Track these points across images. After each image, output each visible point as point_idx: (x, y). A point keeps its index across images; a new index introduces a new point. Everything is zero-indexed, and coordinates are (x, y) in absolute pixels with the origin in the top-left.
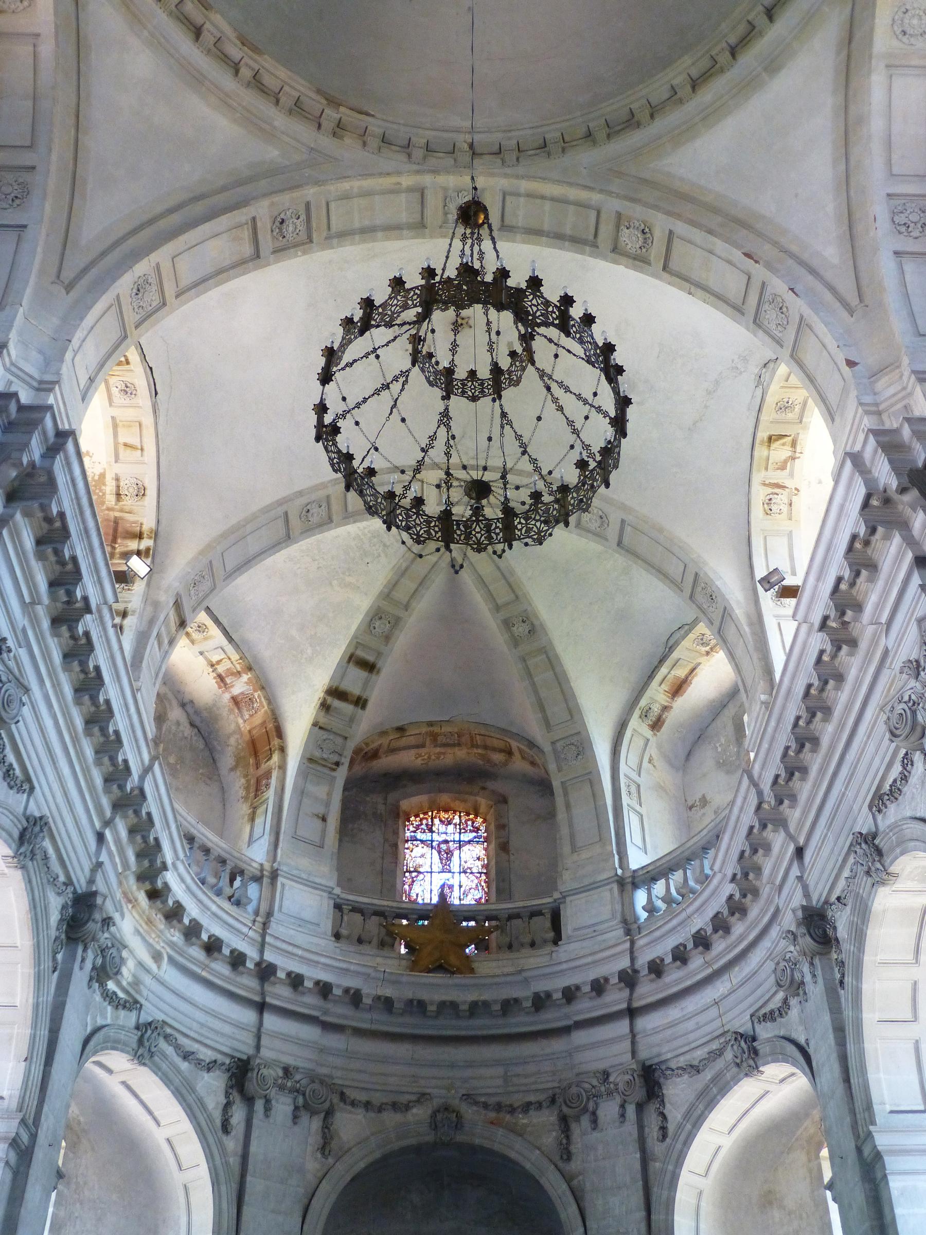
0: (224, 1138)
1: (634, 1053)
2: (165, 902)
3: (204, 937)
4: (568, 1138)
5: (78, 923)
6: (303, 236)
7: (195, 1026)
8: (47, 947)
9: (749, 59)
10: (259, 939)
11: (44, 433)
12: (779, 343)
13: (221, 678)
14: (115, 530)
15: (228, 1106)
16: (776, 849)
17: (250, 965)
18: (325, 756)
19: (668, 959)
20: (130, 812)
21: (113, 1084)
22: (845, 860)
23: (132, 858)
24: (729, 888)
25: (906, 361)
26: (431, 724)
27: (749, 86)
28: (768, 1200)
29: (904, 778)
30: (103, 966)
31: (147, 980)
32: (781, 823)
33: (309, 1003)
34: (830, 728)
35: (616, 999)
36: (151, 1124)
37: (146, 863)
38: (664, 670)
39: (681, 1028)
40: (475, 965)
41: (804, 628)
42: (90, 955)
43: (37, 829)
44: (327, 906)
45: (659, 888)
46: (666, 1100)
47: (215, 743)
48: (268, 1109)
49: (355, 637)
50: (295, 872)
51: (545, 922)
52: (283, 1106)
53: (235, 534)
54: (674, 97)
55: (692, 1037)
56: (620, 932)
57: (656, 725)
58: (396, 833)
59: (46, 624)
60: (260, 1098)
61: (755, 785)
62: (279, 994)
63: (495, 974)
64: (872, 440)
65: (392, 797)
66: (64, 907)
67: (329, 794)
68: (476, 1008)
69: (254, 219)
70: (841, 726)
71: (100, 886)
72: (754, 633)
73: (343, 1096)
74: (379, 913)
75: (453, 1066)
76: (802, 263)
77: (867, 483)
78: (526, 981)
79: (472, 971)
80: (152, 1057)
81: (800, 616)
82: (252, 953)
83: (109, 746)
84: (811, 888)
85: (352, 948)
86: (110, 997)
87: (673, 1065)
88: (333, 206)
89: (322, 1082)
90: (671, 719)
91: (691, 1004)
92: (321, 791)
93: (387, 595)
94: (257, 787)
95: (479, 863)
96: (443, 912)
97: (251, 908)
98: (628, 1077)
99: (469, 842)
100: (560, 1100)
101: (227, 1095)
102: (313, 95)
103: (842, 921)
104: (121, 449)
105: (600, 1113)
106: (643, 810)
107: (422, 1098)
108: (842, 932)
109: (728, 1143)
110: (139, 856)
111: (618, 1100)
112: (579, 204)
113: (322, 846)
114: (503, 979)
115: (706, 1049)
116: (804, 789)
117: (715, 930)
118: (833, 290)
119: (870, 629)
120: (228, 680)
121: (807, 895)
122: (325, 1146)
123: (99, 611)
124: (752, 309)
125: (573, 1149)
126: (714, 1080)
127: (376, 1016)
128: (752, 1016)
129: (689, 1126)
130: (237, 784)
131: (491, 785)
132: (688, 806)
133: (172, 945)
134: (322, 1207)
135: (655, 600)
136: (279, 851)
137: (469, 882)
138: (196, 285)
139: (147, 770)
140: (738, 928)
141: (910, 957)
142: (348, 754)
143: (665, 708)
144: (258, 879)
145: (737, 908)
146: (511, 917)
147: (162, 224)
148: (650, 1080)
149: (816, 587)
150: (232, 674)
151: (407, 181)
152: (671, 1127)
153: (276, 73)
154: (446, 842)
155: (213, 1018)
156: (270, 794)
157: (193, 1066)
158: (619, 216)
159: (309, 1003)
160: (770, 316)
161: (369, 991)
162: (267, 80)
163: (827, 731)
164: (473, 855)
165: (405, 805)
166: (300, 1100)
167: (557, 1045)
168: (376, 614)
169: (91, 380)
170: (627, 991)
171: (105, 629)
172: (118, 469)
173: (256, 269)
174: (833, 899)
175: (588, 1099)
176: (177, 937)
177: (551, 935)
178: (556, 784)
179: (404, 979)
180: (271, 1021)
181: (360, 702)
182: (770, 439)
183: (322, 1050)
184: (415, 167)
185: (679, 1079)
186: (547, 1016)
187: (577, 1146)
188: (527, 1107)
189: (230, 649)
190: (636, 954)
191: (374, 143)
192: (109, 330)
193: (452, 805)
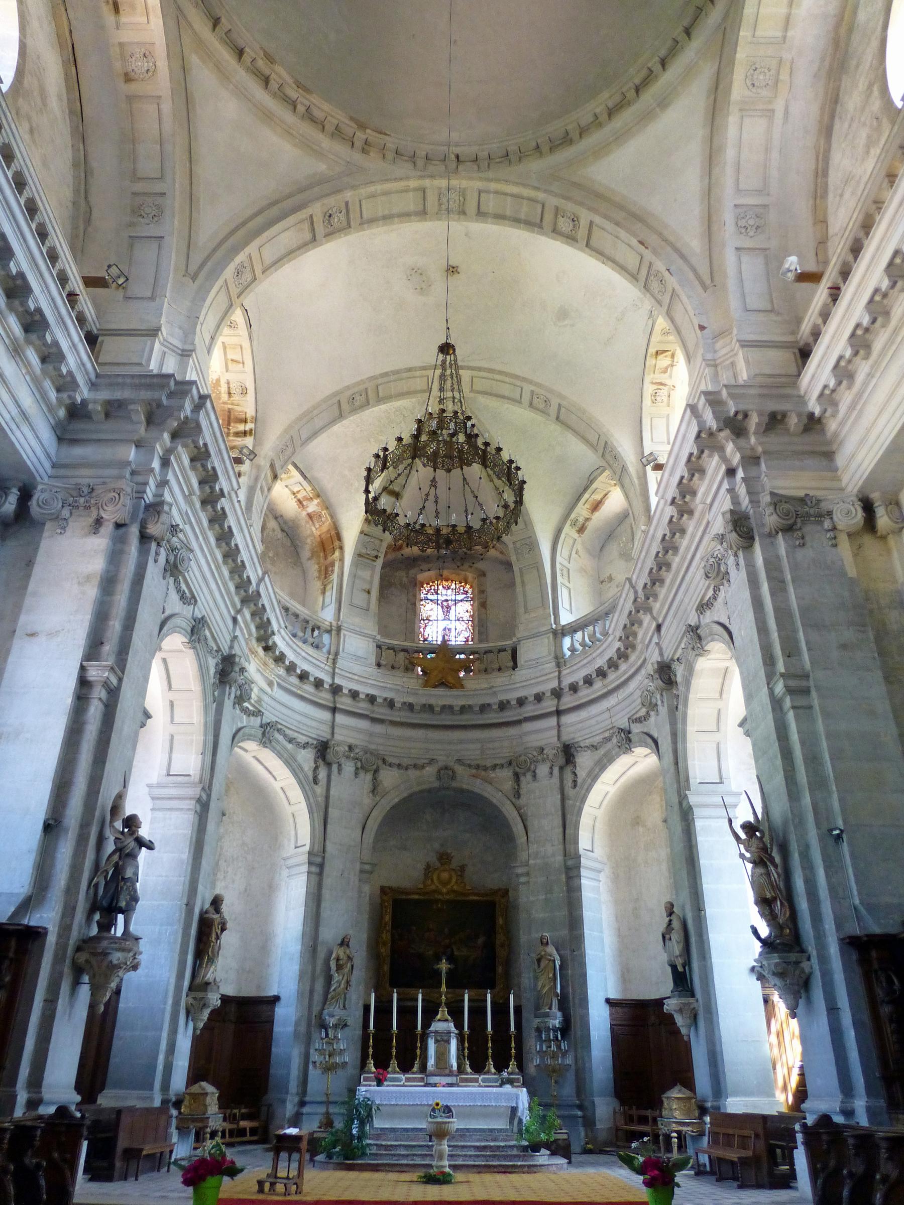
0: (315, 787)
1: (559, 737)
2: (274, 652)
3: (298, 671)
4: (518, 785)
5: (226, 672)
6: (345, 223)
7: (295, 723)
8: (209, 689)
9: (648, 97)
10: (331, 670)
11: (192, 397)
12: (659, 303)
13: (300, 501)
14: (229, 417)
15: (316, 768)
16: (645, 624)
17: (326, 686)
19: (581, 683)
20: (252, 605)
21: (248, 758)
22: (682, 638)
25: (735, 332)
27: (648, 116)
28: (637, 821)
29: (715, 599)
31: (266, 698)
33: (362, 707)
34: (677, 559)
35: (549, 705)
37: (262, 632)
38: (586, 496)
40: (464, 682)
41: (662, 502)
43: (201, 625)
44: (372, 647)
45: (578, 636)
50: (352, 627)
51: (508, 656)
52: (349, 768)
53: (307, 416)
54: (597, 123)
56: (554, 664)
57: (581, 530)
58: (415, 596)
59: (198, 505)
62: (344, 702)
63: (476, 687)
64: (703, 397)
66: (217, 665)
67: (372, 576)
68: (464, 709)
69: (311, 216)
70: (683, 559)
71: (237, 650)
72: (640, 485)
73: (384, 761)
74: (405, 650)
76: (677, 250)
77: (699, 423)
79: (462, 686)
81: (660, 494)
82: (327, 679)
83: (238, 569)
84: (664, 649)
85: (388, 673)
86: (245, 711)
87: (582, 744)
88: (363, 202)
89: (371, 753)
90: (590, 526)
91: (594, 709)
92: (366, 574)
94: (326, 572)
95: (468, 614)
96: (444, 650)
97: (325, 650)
99: (461, 601)
100: (514, 763)
101: (316, 762)
102: (347, 122)
103: (679, 671)
104: (230, 363)
105: (537, 771)
106: (570, 586)
107: (432, 761)
108: (679, 679)
109: (613, 790)
110: (258, 628)
111: (549, 764)
112: (530, 199)
114: (480, 692)
117: (609, 668)
118: (694, 270)
119: (700, 507)
120: (305, 503)
122: (374, 791)
123: (229, 494)
124: (643, 278)
125: (522, 792)
126: (605, 755)
127: (403, 713)
129: (589, 781)
130: (313, 569)
132: (601, 581)
133: (279, 676)
135: (582, 455)
137: (461, 626)
138: (275, 263)
140: (623, 667)
141: (717, 695)
142: (383, 550)
143: (587, 519)
144: (329, 632)
146: (486, 652)
147: (251, 225)
148: (568, 753)
149: (669, 479)
150: (307, 499)
151: (413, 184)
152: (579, 780)
153: (323, 108)
154: (447, 601)
155: (305, 718)
156: (335, 577)
158: (557, 209)
159: (362, 707)
160: (655, 285)
161: (399, 699)
162: (316, 113)
163: (676, 561)
164: (464, 609)
165: (421, 577)
166: (359, 764)
167: (513, 731)
169: (212, 338)
170: (555, 702)
171: (233, 504)
172: (228, 376)
173: (314, 247)
174: (676, 658)
176: (282, 671)
177: (512, 663)
178: (515, 569)
179: (420, 692)
180: (340, 718)
182: (657, 353)
183: (371, 735)
184: (418, 173)
186: (507, 714)
188: (494, 767)
189: (305, 483)
191: (390, 155)
192: (222, 299)
193: (451, 577)
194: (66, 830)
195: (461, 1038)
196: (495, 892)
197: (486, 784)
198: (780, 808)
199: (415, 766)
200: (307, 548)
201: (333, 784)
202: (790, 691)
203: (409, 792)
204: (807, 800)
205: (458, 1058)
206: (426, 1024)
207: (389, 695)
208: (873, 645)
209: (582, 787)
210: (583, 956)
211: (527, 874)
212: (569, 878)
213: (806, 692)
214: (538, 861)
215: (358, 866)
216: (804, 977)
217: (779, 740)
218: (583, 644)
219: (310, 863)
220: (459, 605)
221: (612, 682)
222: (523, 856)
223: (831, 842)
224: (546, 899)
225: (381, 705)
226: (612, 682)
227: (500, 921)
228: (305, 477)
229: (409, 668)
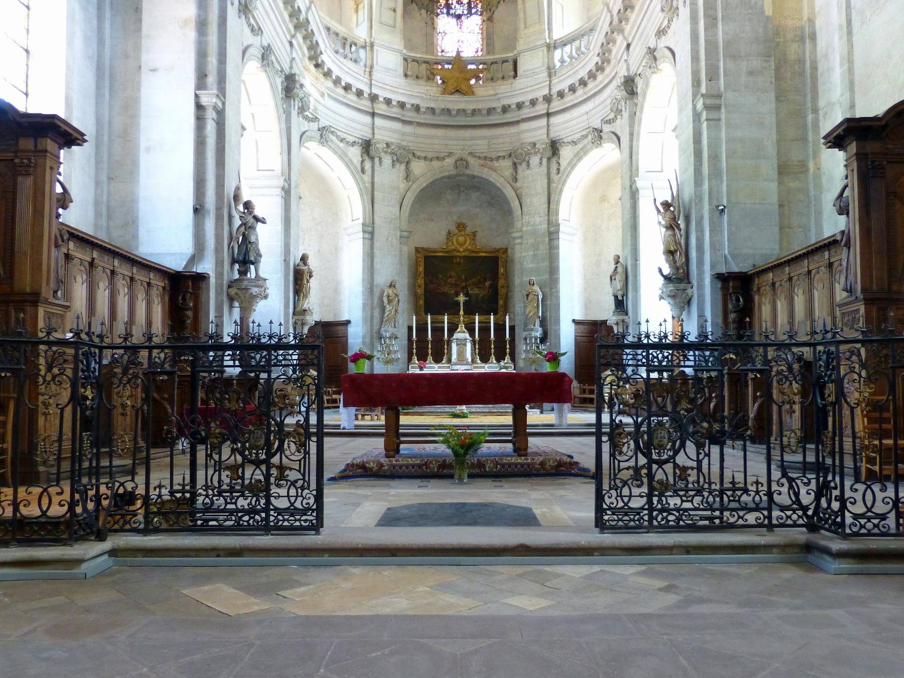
1: (548, 134)
2: (323, 69)
15: (363, 161)
17: (366, 95)
19: (567, 91)
24: (597, 59)
28: (604, 199)
31: (320, 107)
32: (621, 31)
33: (395, 111)
35: (541, 108)
37: (313, 53)
40: (474, 90)
42: (296, 102)
44: (400, 60)
45: (567, 48)
48: (381, 162)
51: (510, 66)
52: (387, 160)
56: (546, 74)
61: (610, 12)
62: (381, 108)
68: (474, 112)
74: (427, 62)
75: (464, 139)
78: (499, 99)
79: (473, 93)
82: (366, 90)
85: (414, 82)
86: (306, 118)
87: (565, 140)
96: (458, 61)
100: (513, 155)
101: (362, 156)
105: (531, 162)
107: (450, 154)
113: (394, 27)
115: (581, 134)
116: (632, 16)
117: (589, 78)
121: (628, 70)
122: (407, 178)
125: (518, 177)
127: (427, 117)
133: (328, 88)
134: (408, 203)
139: (309, 9)
145: (600, 68)
146: (492, 63)
148: (554, 147)
152: (562, 169)
155: (353, 123)
159: (395, 111)
161: (423, 105)
166: (395, 158)
167: (513, 130)
176: (330, 84)
177: (513, 73)
180: (378, 121)
183: (403, 134)
186: (506, 116)
187: (519, 177)
194: (209, 212)
195: (474, 342)
196: (498, 250)
197: (491, 172)
198: (688, 192)
199: (438, 158)
201: (376, 173)
202: (707, 107)
203: (434, 178)
204: (706, 186)
205: (472, 355)
206: (451, 334)
207: (416, 101)
208: (773, 72)
209: (564, 172)
210: (558, 292)
211: (521, 237)
212: (551, 240)
213: (718, 108)
214: (529, 228)
215: (398, 234)
216: (688, 298)
217: (694, 143)
218: (571, 57)
219: (364, 232)
221: (591, 90)
222: (518, 224)
223: (717, 214)
224: (535, 255)
225: (410, 110)
226: (591, 90)
227: (502, 270)
229: (431, 77)
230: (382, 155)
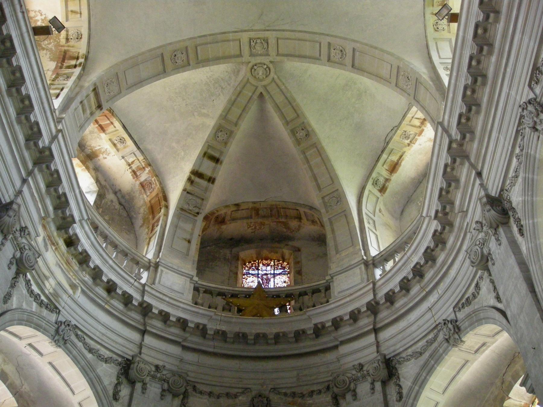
0: (114, 403)
2: (76, 249)
10: (141, 288)
13: (134, 172)
15: (118, 384)
17: (135, 303)
18: (191, 208)
23: (51, 208)
26: (254, 203)
30: (21, 258)
36: (70, 393)
38: (384, 156)
39: (408, 331)
45: (389, 265)
46: (401, 377)
47: (133, 214)
49: (207, 142)
52: (154, 389)
53: (133, 63)
55: (414, 335)
57: (383, 190)
60: (139, 382)
65: (235, 250)
67: (193, 229)
68: (278, 338)
74: (221, 294)
78: (310, 318)
80: (65, 343)
82: (137, 296)
87: (404, 355)
89: (180, 376)
90: (391, 187)
92: (188, 227)
93: (224, 117)
98: (376, 365)
101: (118, 378)
105: (358, 391)
111: (370, 379)
120: (138, 173)
126: (431, 356)
128: (454, 308)
131: (290, 243)
133: (84, 282)
136: (161, 254)
143: (387, 180)
150: (140, 169)
152: (405, 392)
156: (158, 229)
157: (95, 357)
166: (166, 386)
167: (330, 356)
168: (219, 129)
170: (373, 317)
175: (350, 383)
176: (88, 279)
180: (148, 340)
181: (212, 180)
185: (408, 363)
188: (311, 393)
189: (138, 153)
190: (377, 292)
193: (269, 255)
199: (228, 395)
200: (140, 216)
220: (277, 277)
228: (138, 148)
230: (148, 379)
